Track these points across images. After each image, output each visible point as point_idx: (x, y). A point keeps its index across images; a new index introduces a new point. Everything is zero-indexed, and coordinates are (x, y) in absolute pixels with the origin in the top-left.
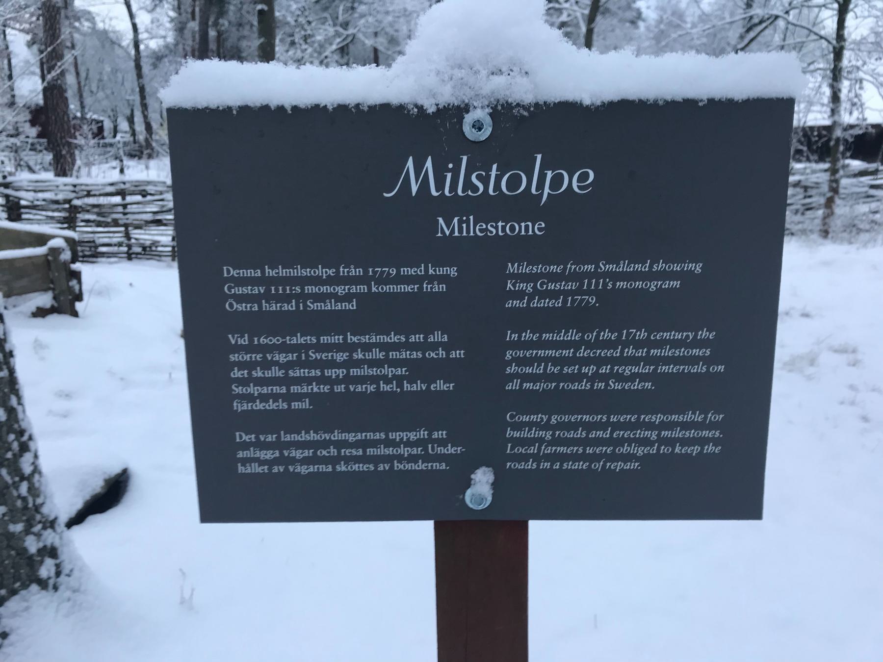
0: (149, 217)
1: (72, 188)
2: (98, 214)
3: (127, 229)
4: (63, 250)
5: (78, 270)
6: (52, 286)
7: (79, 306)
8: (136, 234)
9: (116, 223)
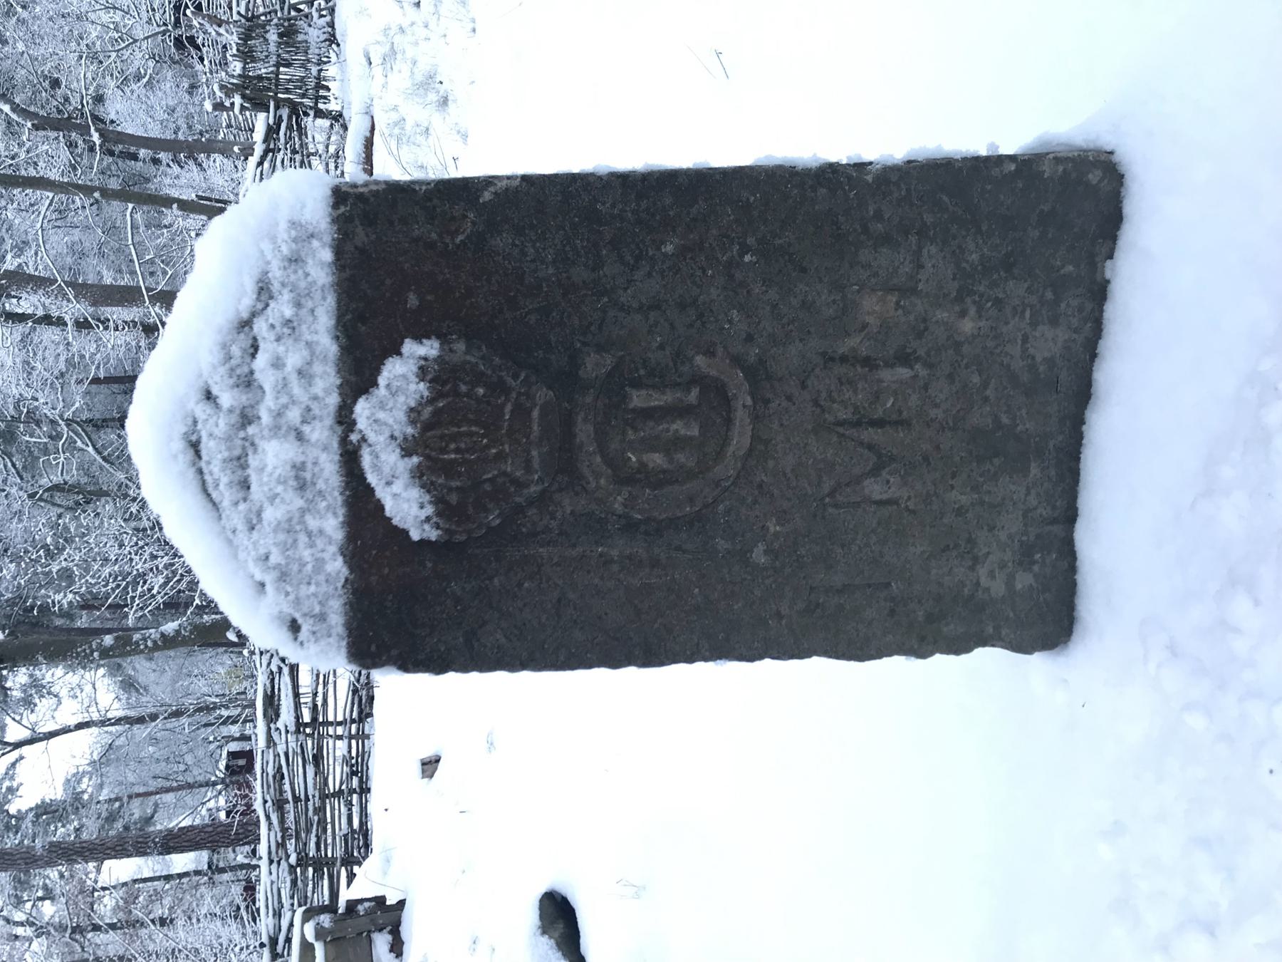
0: (311, 770)
1: (274, 866)
2: (308, 831)
3: (327, 796)
4: (318, 924)
5: (344, 905)
6: (365, 934)
7: (391, 901)
8: (333, 784)
9: (320, 810)
